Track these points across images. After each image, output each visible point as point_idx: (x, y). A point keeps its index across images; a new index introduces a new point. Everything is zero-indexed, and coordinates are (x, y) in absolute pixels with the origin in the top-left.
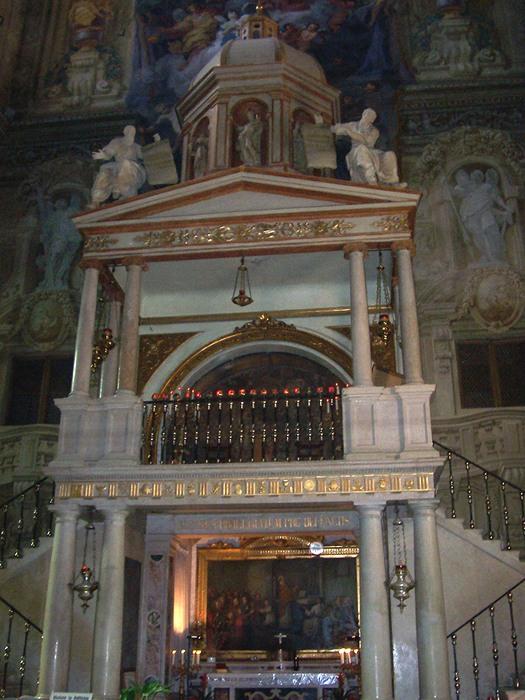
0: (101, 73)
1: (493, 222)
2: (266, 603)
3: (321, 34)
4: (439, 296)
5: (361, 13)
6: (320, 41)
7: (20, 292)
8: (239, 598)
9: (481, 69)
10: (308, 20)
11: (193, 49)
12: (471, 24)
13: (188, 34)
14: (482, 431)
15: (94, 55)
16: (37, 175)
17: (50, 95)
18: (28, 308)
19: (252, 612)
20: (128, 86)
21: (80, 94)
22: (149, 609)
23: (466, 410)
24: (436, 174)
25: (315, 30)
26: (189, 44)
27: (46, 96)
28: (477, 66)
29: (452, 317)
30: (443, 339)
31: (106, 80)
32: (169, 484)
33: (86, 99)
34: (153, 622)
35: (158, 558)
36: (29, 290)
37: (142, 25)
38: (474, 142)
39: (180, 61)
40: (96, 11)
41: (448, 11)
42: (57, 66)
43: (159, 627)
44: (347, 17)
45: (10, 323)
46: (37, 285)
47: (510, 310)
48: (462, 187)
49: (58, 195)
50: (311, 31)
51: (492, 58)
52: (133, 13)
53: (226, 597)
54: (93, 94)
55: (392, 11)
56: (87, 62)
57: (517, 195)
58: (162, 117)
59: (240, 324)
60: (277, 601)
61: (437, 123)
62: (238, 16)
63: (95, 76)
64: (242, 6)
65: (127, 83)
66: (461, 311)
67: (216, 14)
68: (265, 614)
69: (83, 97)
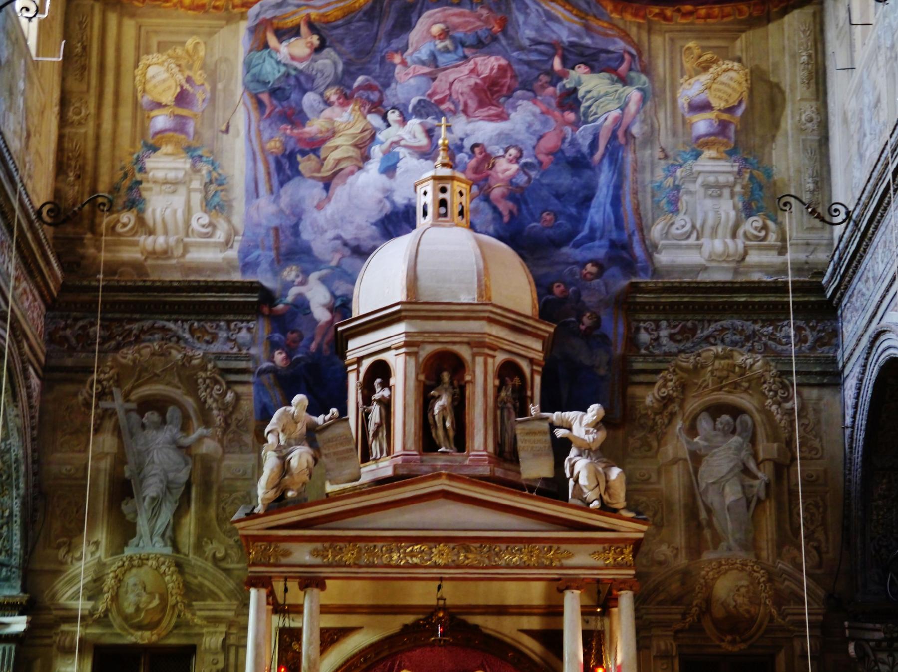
1: (740, 495)
3: (526, 167)
4: (661, 597)
5: (583, 136)
6: (522, 180)
7: (101, 553)
9: (746, 253)
10: (508, 141)
11: (335, 175)
12: (740, 173)
13: (330, 144)
15: (184, 163)
16: (112, 368)
17: (119, 229)
18: (116, 577)
21: (166, 233)
24: (672, 415)
25: (517, 159)
27: (112, 229)
29: (678, 626)
30: (664, 655)
31: (205, 212)
33: (178, 241)
36: (117, 548)
37: (255, 115)
38: (725, 373)
40: (180, 78)
41: (707, 145)
44: (563, 139)
45: (90, 598)
46: (126, 544)
47: (752, 620)
48: (706, 440)
49: (146, 405)
50: (511, 161)
51: (763, 234)
52: (240, 90)
54: (187, 235)
55: (627, 132)
56: (171, 175)
57: (776, 456)
58: (293, 292)
59: (409, 619)
61: (679, 337)
62: (404, 121)
63: (188, 202)
64: (409, 101)
65: (238, 220)
66: (689, 619)
67: (369, 112)
69: (172, 240)
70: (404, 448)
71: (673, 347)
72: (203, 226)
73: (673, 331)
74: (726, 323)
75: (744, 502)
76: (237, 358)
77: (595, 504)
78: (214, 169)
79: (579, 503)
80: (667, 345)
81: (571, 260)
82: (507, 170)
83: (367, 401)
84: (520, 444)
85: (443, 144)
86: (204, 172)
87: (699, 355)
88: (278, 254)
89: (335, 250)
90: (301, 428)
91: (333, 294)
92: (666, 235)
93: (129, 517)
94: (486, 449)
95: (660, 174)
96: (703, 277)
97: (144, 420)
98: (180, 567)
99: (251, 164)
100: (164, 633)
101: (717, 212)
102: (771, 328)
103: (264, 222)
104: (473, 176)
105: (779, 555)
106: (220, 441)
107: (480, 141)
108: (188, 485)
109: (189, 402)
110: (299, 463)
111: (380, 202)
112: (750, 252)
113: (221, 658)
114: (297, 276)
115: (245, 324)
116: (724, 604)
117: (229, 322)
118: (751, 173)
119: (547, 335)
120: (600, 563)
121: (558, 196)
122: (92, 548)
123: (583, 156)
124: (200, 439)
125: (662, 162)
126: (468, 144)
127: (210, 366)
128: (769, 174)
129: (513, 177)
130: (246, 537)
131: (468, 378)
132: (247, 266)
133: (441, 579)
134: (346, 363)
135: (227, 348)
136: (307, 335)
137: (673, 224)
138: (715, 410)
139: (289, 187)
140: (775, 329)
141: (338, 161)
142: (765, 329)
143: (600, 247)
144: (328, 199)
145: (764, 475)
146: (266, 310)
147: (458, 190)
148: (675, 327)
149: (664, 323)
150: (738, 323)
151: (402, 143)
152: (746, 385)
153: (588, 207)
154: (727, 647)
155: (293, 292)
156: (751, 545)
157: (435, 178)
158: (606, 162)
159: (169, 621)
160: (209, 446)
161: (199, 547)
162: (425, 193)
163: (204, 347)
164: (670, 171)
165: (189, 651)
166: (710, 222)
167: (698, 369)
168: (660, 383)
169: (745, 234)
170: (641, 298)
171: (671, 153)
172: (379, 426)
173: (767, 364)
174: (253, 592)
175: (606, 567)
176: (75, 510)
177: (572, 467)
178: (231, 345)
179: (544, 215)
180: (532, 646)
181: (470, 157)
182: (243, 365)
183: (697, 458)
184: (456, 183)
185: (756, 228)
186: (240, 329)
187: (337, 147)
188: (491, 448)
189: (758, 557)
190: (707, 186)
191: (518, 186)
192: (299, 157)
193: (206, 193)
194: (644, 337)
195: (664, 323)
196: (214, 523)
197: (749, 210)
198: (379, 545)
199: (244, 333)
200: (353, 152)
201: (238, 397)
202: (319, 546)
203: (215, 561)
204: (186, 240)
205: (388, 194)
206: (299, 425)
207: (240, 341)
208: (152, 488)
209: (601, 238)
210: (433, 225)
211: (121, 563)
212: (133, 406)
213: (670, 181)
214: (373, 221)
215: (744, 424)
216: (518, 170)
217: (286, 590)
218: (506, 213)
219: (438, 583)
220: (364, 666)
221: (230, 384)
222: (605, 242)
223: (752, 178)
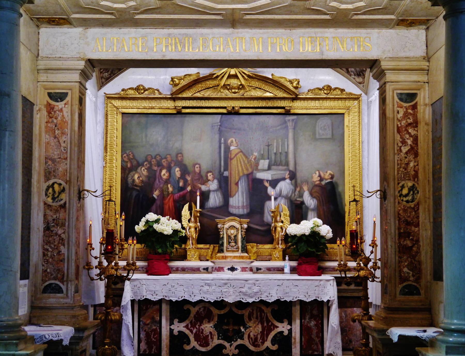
2: (210, 176)
8: (169, 169)
19: (189, 189)
22: (47, 178)
34: (53, 199)
35: (60, 97)
43: (63, 206)
53: (149, 169)
60: (226, 174)
68: (209, 192)
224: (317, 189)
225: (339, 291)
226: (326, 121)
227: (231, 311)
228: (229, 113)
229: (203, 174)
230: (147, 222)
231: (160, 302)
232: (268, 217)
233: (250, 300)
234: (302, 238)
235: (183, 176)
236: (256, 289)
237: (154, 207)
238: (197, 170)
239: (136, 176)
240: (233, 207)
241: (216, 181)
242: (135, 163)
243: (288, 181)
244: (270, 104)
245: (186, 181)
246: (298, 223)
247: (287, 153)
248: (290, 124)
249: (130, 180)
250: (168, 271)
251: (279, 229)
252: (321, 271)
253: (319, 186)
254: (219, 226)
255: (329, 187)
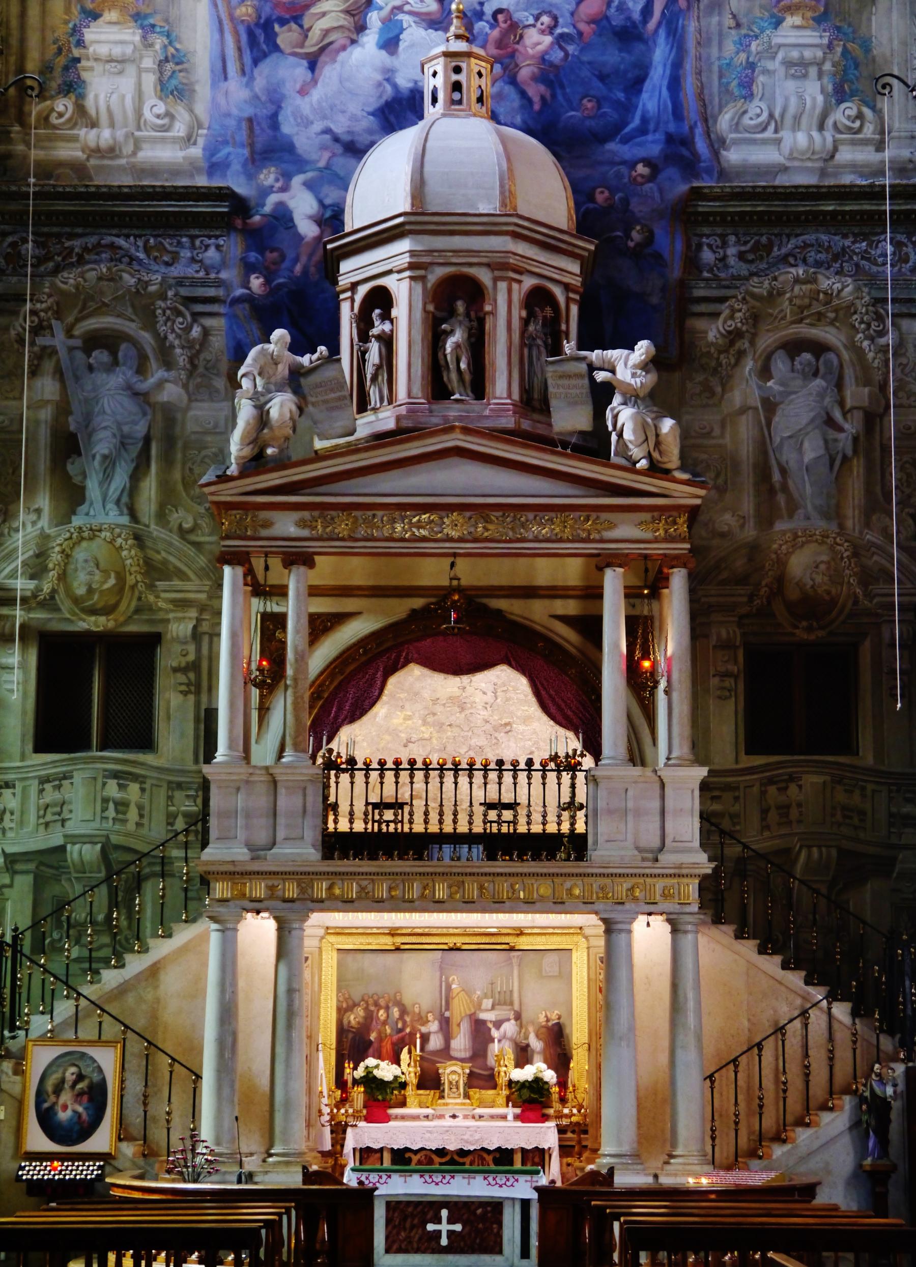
0: (150, 81)
1: (822, 451)
4: (725, 575)
6: (557, 56)
7: (44, 522)
8: (387, 1008)
9: (836, 149)
11: (322, 49)
12: (830, 46)
13: (314, 10)
14: (772, 790)
15: (132, 35)
16: (50, 296)
17: (54, 120)
18: (63, 552)
19: (408, 1030)
20: (206, 121)
21: (112, 125)
23: (752, 757)
24: (741, 354)
25: (551, 30)
26: (315, 34)
27: (45, 120)
28: (829, 140)
30: (726, 646)
31: (161, 99)
32: (364, 883)
33: (127, 136)
36: (64, 517)
38: (807, 301)
39: (301, 71)
42: (60, 51)
45: (32, 577)
46: (74, 513)
48: (782, 384)
49: (93, 341)
50: (542, 32)
51: (857, 124)
53: (366, 1009)
54: (139, 128)
56: (117, 51)
57: (866, 404)
58: (272, 199)
59: (418, 603)
60: (447, 1014)
61: (751, 257)
65: (201, 108)
66: (757, 602)
68: (429, 1034)
69: (120, 134)
70: (409, 396)
71: (743, 269)
72: (158, 116)
73: (743, 248)
74: (809, 238)
75: (826, 460)
76: (204, 283)
77: (643, 464)
78: (170, 43)
79: (622, 462)
80: (736, 267)
81: (617, 159)
82: (539, 44)
83: (364, 337)
84: (551, 389)
85: (458, 10)
86: (158, 47)
87: (775, 279)
88: (253, 152)
89: (323, 148)
90: (282, 371)
91: (321, 202)
92: (736, 126)
93: (77, 480)
94: (509, 396)
95: (730, 47)
96: (782, 180)
97: (91, 360)
98: (139, 539)
99: (217, 36)
100: (122, 619)
101: (801, 98)
102: (864, 244)
103: (235, 111)
104: (494, 51)
105: (867, 524)
106: (185, 386)
107: (504, 7)
108: (147, 440)
109: (146, 338)
110: (281, 414)
111: (380, 84)
112: (841, 148)
113: (191, 648)
114: (277, 180)
115: (213, 241)
116: (800, 585)
117: (193, 238)
118: (844, 45)
119: (586, 254)
120: (648, 535)
121: (602, 78)
122: (33, 517)
123: (634, 23)
124: (160, 385)
125: (733, 32)
126: (489, 9)
127: (170, 294)
128: (867, 50)
129: (546, 52)
130: (217, 504)
131: (488, 308)
132: (214, 167)
133: (455, 555)
134: (338, 289)
135: (191, 271)
136: (290, 255)
137: (745, 112)
138: (793, 347)
139: (265, 67)
140: (870, 245)
141: (327, 32)
142: (857, 245)
143: (653, 142)
144: (315, 82)
145: (852, 427)
146: (239, 223)
147: (476, 69)
148: (746, 243)
149: (732, 239)
150: (824, 237)
151: (407, 8)
152: (832, 315)
153: (640, 91)
154: (802, 635)
155: (272, 199)
156: (834, 513)
157: (446, 54)
158: (662, 32)
159: (127, 605)
160: (172, 393)
161: (161, 517)
162: (435, 74)
163: (163, 269)
164: (743, 45)
165: (154, 640)
166: (792, 110)
167: (773, 296)
168: (727, 312)
169: (835, 123)
170: (704, 206)
171: (744, 21)
172: (378, 368)
173: (858, 289)
174: (227, 570)
175: (656, 540)
176: (11, 471)
177: (615, 417)
178: (196, 267)
179: (585, 101)
180: (568, 635)
181: (492, 27)
182: (211, 292)
183: (770, 406)
184: (473, 61)
185: (849, 117)
186: (207, 247)
187: (324, 14)
188: (516, 396)
189: (841, 526)
190: (788, 64)
191: (552, 65)
192: (277, 27)
193: (161, 73)
194: (707, 256)
195: (732, 239)
196: (180, 487)
197: (840, 94)
198: (380, 513)
199: (212, 253)
200: (344, 21)
201: (206, 332)
202: (306, 514)
203: (182, 533)
204: (137, 134)
205: (389, 75)
206: (280, 367)
207: (208, 262)
208: (103, 445)
209: (655, 131)
210: (444, 115)
211: (68, 535)
212: (78, 343)
213: (743, 56)
214: (370, 109)
215: (828, 363)
216: (552, 43)
217: (267, 568)
218: (536, 99)
219: (451, 559)
220: (364, 659)
221: (196, 316)
222: (660, 136)
223: (845, 52)
224: (544, 1030)
225: (560, 1140)
226: (554, 957)
227: (452, 1158)
228: (451, 949)
229: (423, 1014)
230: (367, 1067)
231: (381, 1150)
232: (491, 1061)
233: (472, 1148)
234: (523, 1085)
235: (401, 1017)
236: (477, 1136)
237: (371, 1051)
238: (417, 1010)
239: (352, 1017)
240: (455, 1050)
241: (436, 1023)
242: (351, 1003)
243: (513, 1022)
244: (494, 940)
245: (405, 1023)
246: (522, 1067)
247: (511, 992)
248: (515, 961)
249: (345, 1022)
250: (386, 1119)
251: (502, 1074)
252: (545, 1118)
253: (546, 1027)
254: (440, 1071)
255: (556, 1028)
